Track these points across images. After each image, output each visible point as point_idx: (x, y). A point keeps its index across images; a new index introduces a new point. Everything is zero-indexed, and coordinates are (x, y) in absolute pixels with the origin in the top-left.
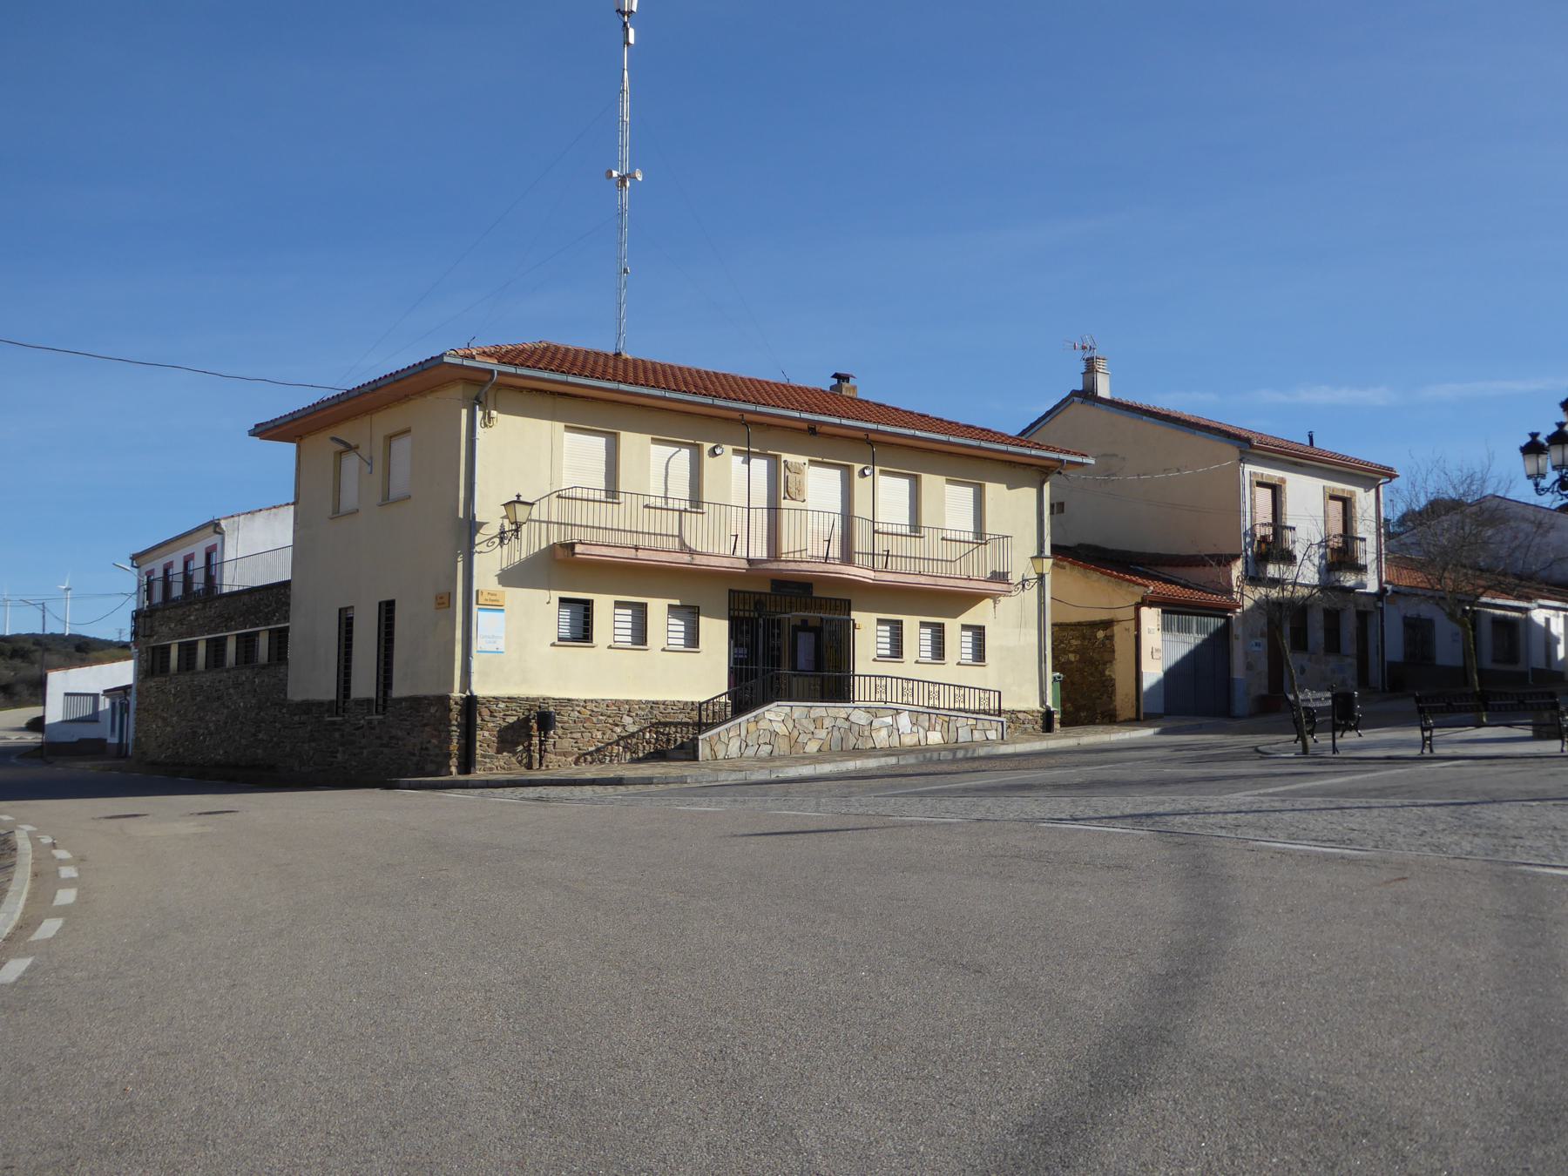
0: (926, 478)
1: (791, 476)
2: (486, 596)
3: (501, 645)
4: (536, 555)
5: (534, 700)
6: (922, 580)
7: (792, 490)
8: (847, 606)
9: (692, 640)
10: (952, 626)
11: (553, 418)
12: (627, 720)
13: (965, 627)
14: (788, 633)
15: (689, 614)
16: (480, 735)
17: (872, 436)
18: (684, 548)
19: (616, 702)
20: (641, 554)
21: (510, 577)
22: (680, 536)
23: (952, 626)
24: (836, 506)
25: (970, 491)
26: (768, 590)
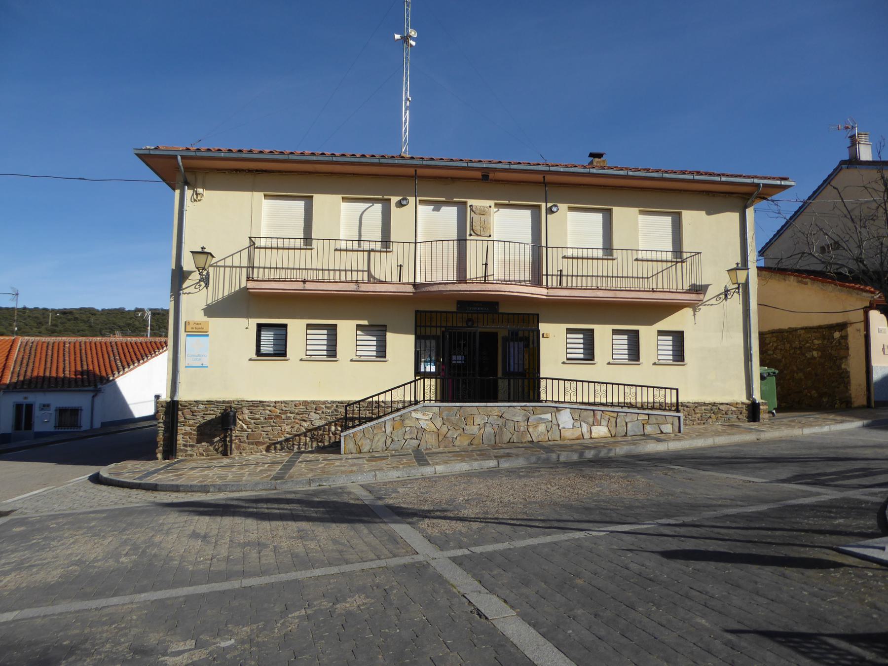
0: (619, 212)
1: (476, 218)
2: (192, 325)
3: (205, 361)
4: (236, 293)
5: (228, 402)
6: (600, 294)
7: (477, 228)
8: (535, 319)
9: (382, 352)
10: (648, 334)
11: (252, 189)
12: (313, 416)
13: (661, 333)
14: (479, 346)
15: (378, 331)
16: (182, 429)
17: (549, 178)
18: (372, 279)
19: (306, 403)
20: (308, 286)
21: (212, 311)
22: (369, 271)
23: (648, 334)
24: (528, 238)
25: (668, 220)
26: (454, 309)
